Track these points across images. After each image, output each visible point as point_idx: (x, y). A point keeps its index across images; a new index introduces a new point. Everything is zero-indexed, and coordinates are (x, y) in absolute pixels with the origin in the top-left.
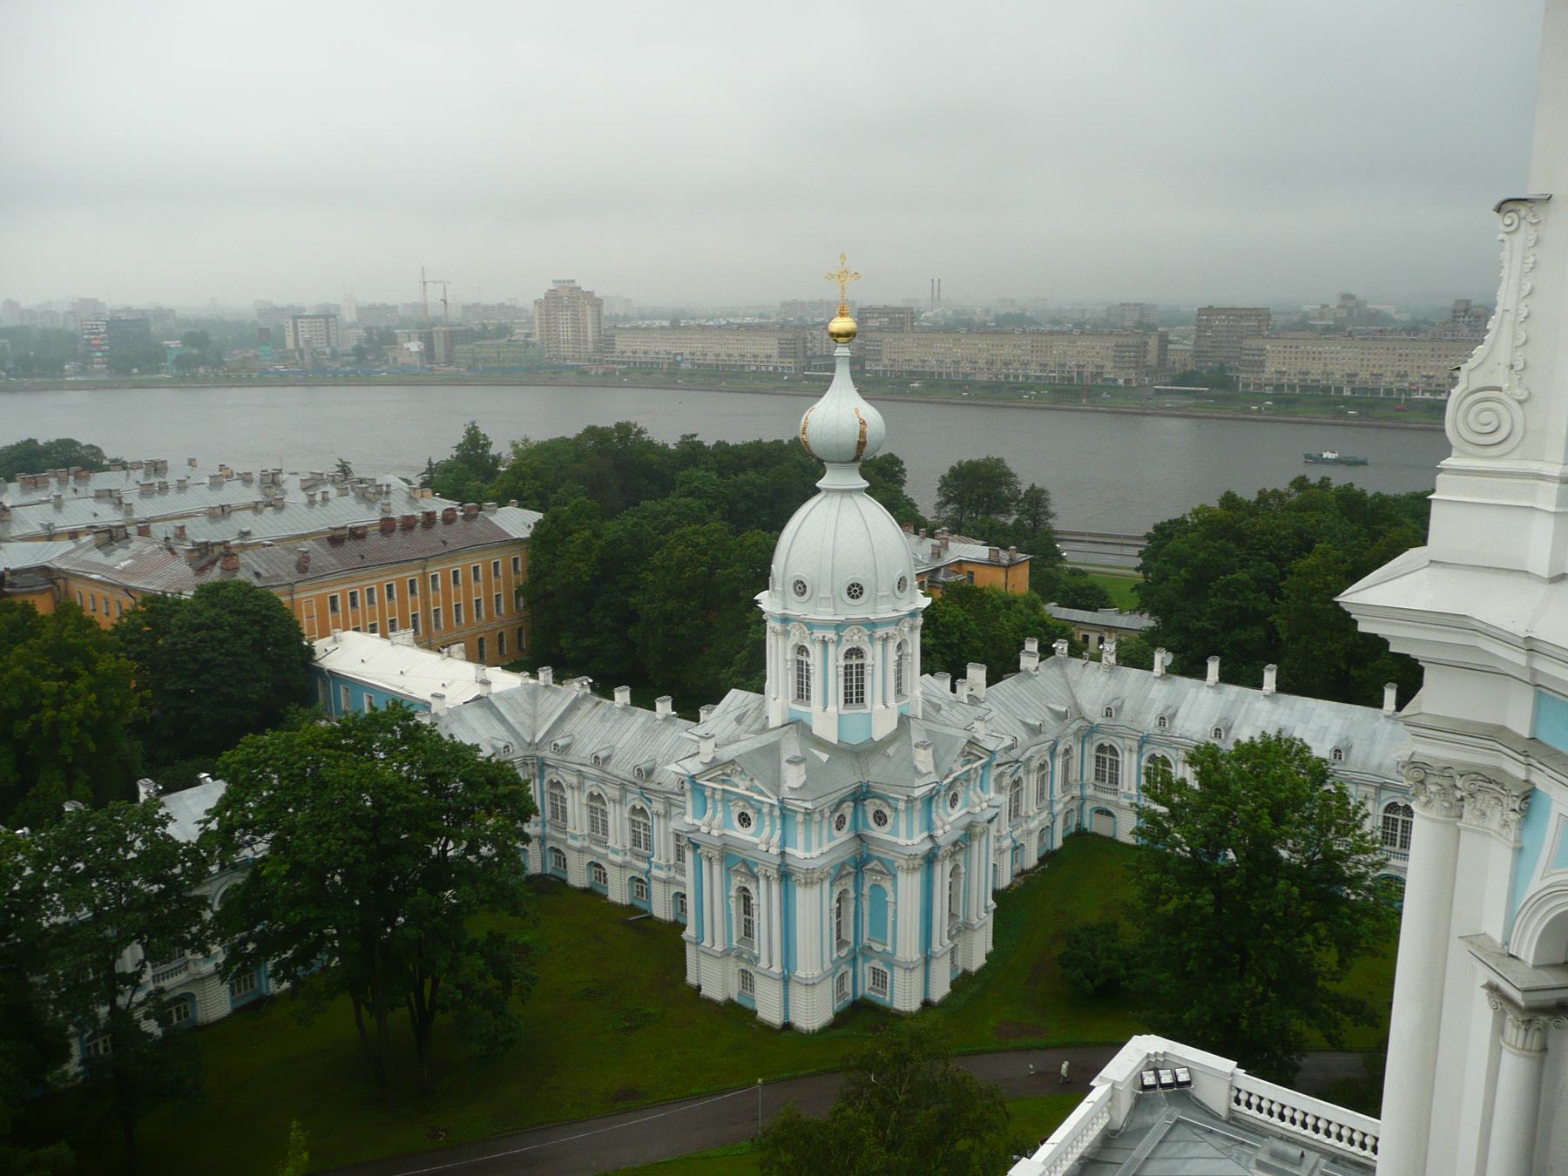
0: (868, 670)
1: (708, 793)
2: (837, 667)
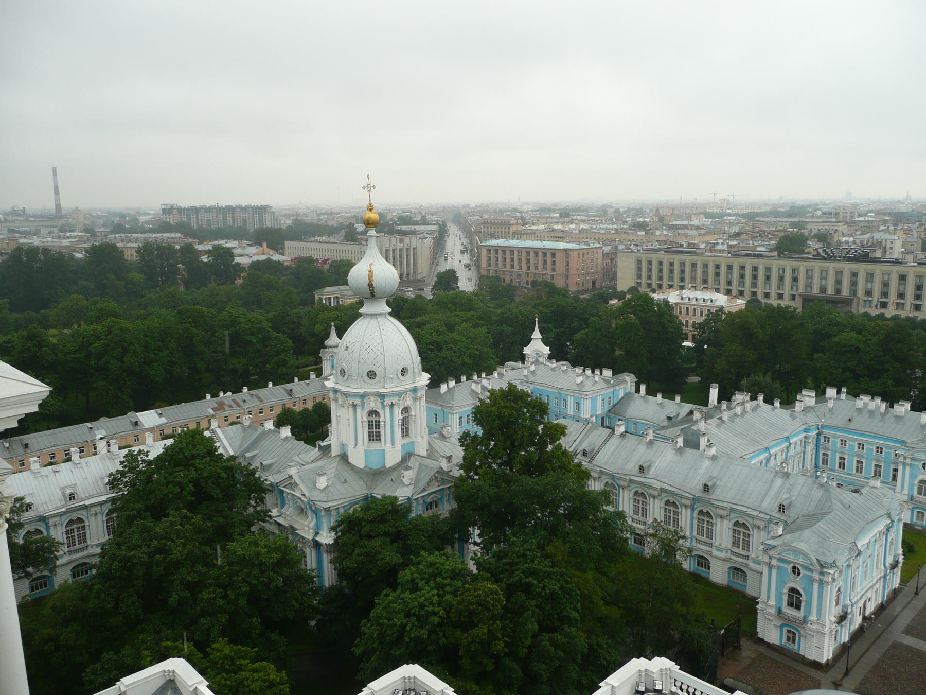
0: (382, 424)
2: (362, 422)
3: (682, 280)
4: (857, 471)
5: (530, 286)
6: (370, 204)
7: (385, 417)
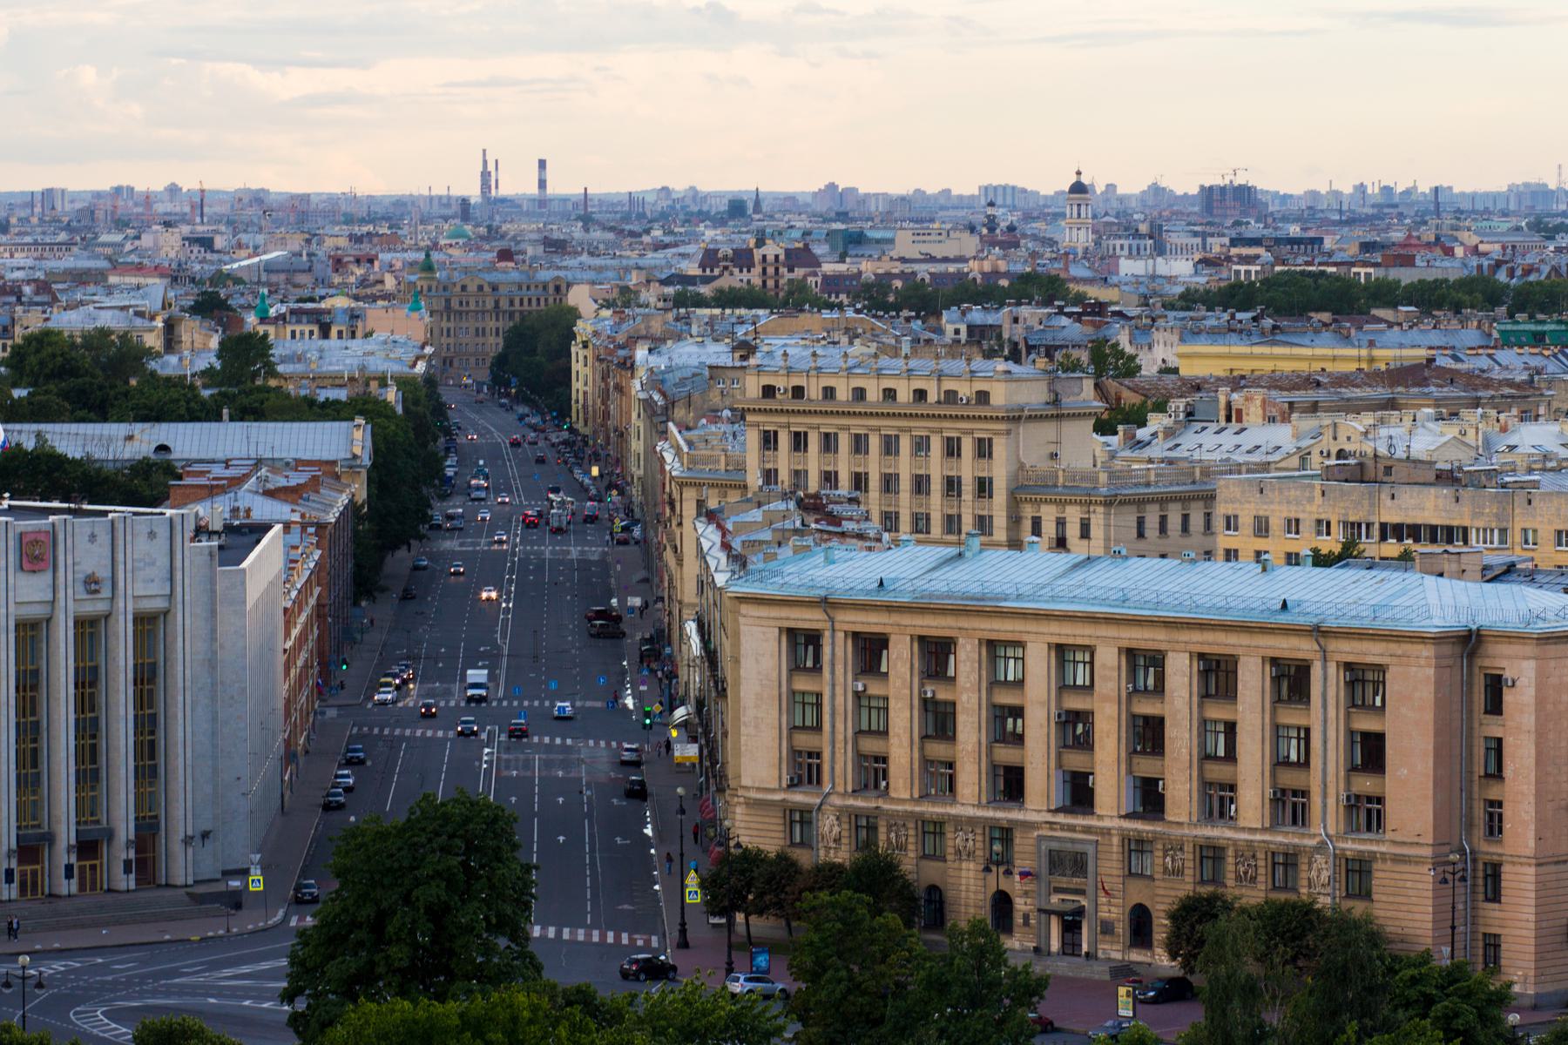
5: (1162, 961)
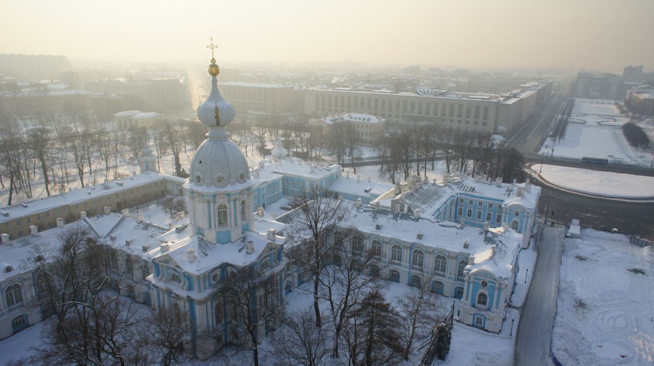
1: (160, 267)
3: (349, 107)
4: (497, 221)
6: (213, 59)
7: (230, 207)
